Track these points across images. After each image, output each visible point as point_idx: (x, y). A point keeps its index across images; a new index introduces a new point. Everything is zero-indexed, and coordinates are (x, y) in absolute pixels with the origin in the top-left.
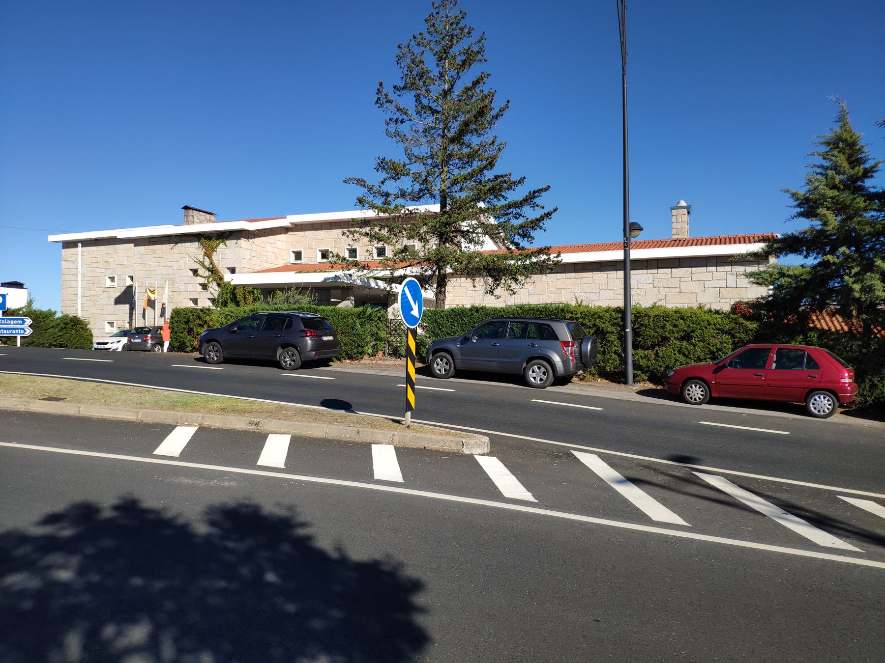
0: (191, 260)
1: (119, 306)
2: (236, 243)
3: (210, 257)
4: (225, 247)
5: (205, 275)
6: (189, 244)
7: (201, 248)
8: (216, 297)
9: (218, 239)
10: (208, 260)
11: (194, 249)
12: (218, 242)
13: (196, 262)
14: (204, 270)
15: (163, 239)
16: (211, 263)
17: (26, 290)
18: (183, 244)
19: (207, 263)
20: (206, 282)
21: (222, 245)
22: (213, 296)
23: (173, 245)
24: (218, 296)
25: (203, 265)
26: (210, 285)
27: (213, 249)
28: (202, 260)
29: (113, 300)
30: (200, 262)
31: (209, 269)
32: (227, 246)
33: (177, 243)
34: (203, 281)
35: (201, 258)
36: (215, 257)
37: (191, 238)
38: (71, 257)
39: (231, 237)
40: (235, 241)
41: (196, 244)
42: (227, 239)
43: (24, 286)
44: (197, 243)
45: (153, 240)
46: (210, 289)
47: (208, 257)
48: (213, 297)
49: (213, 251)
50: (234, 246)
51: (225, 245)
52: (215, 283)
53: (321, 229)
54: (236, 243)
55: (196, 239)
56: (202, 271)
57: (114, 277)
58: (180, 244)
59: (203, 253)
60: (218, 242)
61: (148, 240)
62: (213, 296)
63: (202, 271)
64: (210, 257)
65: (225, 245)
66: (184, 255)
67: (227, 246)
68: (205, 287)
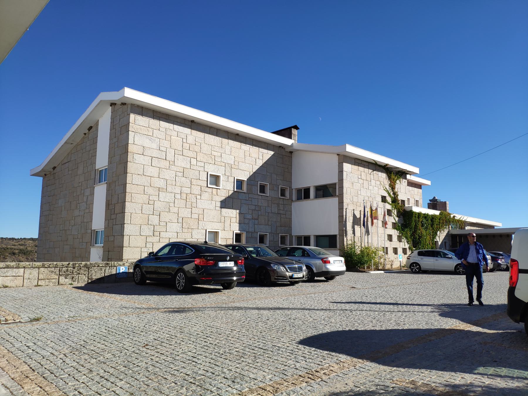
1: (224, 210)
15: (365, 163)
16: (394, 194)
29: (219, 204)
33: (374, 170)
35: (388, 187)
41: (383, 176)
44: (385, 174)
51: (400, 181)
55: (385, 171)
63: (389, 199)
64: (393, 188)
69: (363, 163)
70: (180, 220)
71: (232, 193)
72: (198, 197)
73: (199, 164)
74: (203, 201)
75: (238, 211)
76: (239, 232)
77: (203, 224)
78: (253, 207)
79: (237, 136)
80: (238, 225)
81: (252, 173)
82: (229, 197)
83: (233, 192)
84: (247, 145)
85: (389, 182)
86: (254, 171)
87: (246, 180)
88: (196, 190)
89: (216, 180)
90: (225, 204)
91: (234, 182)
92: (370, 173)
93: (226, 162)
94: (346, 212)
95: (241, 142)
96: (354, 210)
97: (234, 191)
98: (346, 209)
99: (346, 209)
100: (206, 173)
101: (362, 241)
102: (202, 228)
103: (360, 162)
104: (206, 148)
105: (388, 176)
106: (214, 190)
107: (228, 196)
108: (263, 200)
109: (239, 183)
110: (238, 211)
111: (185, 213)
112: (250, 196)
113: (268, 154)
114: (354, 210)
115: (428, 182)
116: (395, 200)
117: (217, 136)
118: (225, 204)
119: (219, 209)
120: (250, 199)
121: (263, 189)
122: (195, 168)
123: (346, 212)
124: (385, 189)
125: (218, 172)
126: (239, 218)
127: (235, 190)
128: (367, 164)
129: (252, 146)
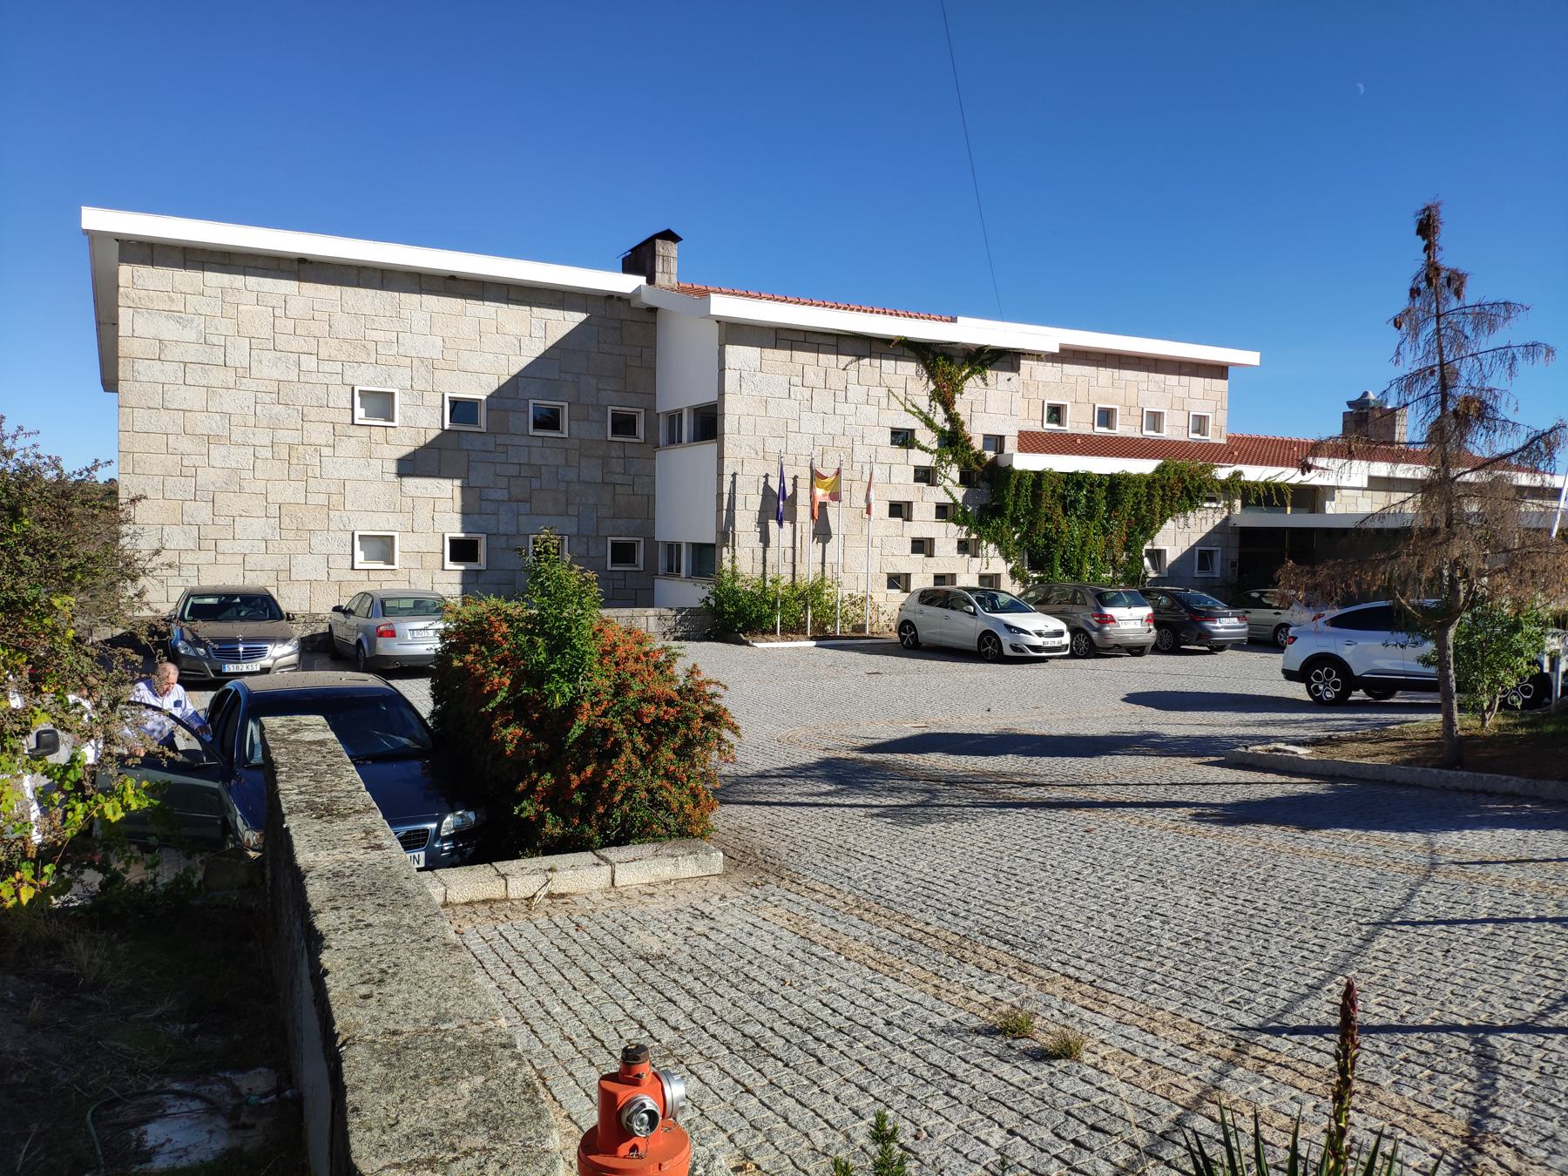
1: (410, 483)
2: (1009, 380)
3: (947, 405)
4: (980, 382)
7: (925, 379)
8: (960, 501)
10: (940, 409)
11: (907, 375)
13: (914, 414)
15: (821, 340)
16: (953, 419)
18: (876, 362)
19: (940, 418)
22: (952, 496)
24: (965, 497)
25: (929, 423)
27: (957, 387)
28: (925, 410)
29: (392, 467)
30: (921, 413)
32: (986, 385)
33: (860, 357)
34: (926, 460)
35: (923, 403)
36: (961, 406)
38: (171, 300)
41: (909, 368)
44: (915, 364)
45: (794, 337)
48: (951, 501)
51: (984, 379)
54: (1009, 380)
55: (913, 354)
57: (392, 394)
61: (772, 335)
62: (952, 496)
63: (926, 437)
64: (947, 405)
65: (984, 379)
67: (986, 385)
68: (925, 476)
70: (274, 510)
71: (438, 437)
72: (326, 451)
73: (326, 367)
74: (341, 460)
75: (458, 482)
76: (462, 535)
77: (345, 520)
78: (513, 470)
79: (452, 283)
80: (459, 516)
81: (506, 378)
82: (428, 447)
83: (438, 432)
84: (487, 303)
85: (932, 387)
86: (515, 370)
87: (484, 398)
88: (319, 434)
89: (381, 404)
90: (410, 466)
91: (443, 407)
92: (842, 366)
93: (414, 354)
94: (734, 482)
95: (465, 296)
96: (766, 476)
97: (443, 429)
98: (734, 475)
99: (734, 475)
100: (349, 389)
101: (798, 559)
102: (342, 528)
104: (343, 325)
105: (927, 367)
106: (378, 434)
107: (422, 444)
108: (548, 450)
109: (462, 409)
110: (458, 482)
111: (288, 492)
113: (566, 321)
114: (766, 476)
115: (1251, 358)
116: (953, 440)
117: (382, 288)
118: (410, 466)
119: (392, 477)
120: (499, 449)
121: (548, 420)
122: (314, 378)
124: (909, 406)
125: (389, 383)
126: (463, 499)
127: (447, 427)
128: (833, 341)
129: (504, 305)
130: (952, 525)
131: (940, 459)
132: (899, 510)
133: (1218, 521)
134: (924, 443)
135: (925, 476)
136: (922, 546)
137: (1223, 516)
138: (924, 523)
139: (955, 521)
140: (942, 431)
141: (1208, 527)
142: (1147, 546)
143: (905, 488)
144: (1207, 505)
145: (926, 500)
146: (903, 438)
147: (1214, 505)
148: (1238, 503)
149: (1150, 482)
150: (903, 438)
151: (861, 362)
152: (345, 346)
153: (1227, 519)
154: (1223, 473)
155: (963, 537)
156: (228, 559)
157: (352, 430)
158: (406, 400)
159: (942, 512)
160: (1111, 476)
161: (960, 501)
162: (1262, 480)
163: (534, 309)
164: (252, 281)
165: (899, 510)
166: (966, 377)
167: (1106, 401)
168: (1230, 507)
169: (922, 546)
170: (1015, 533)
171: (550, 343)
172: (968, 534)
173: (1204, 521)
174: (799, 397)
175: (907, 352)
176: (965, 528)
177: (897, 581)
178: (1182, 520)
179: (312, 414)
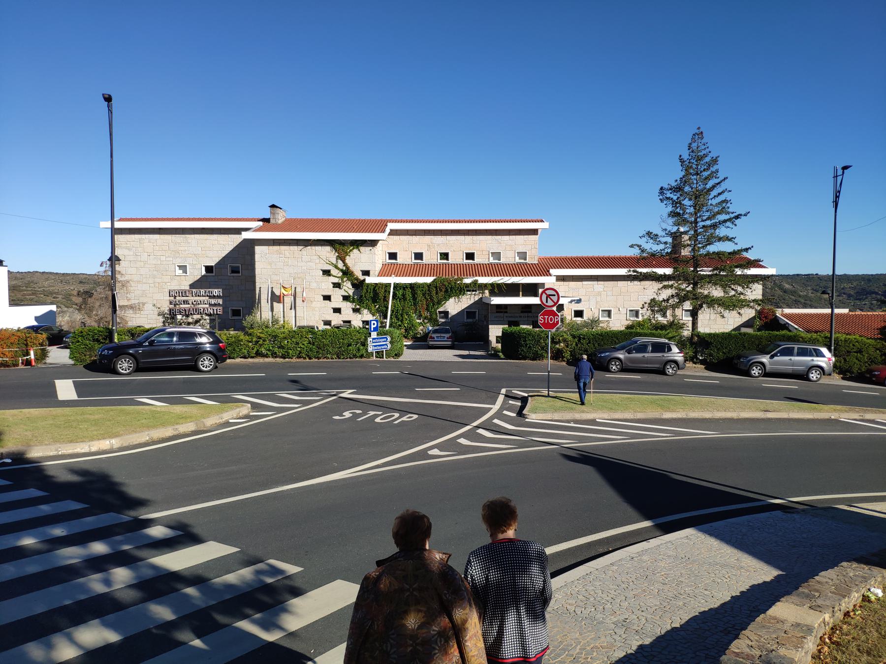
0: (323, 262)
3: (344, 261)
4: (358, 252)
5: (338, 276)
6: (320, 247)
7: (334, 252)
8: (351, 294)
9: (351, 246)
11: (328, 253)
12: (351, 248)
13: (329, 264)
14: (337, 271)
16: (345, 265)
17: (6, 267)
18: (313, 247)
19: (340, 264)
20: (340, 281)
21: (355, 251)
23: (302, 247)
25: (336, 267)
26: (345, 284)
27: (347, 254)
28: (335, 262)
30: (333, 264)
31: (342, 270)
33: (306, 246)
34: (336, 280)
35: (334, 261)
36: (348, 260)
37: (323, 243)
39: (364, 245)
40: (371, 248)
41: (328, 248)
42: (361, 246)
43: (4, 263)
46: (344, 288)
47: (341, 260)
48: (348, 294)
49: (346, 255)
50: (368, 252)
51: (359, 250)
52: (350, 283)
53: (415, 235)
55: (328, 244)
56: (334, 272)
57: (186, 266)
58: (309, 247)
59: (335, 256)
60: (351, 248)
63: (334, 272)
64: (344, 261)
65: (359, 250)
66: (315, 257)
69: (288, 241)
71: (200, 278)
73: (168, 259)
85: (337, 254)
93: (192, 253)
103: (291, 242)
105: (334, 248)
112: (219, 278)
116: (347, 273)
123: (260, 290)
128: (296, 242)
130: (348, 303)
131: (342, 280)
132: (327, 298)
133: (477, 299)
134: (334, 274)
135: (337, 285)
136: (337, 310)
137: (479, 297)
138: (337, 301)
139: (350, 302)
140: (342, 270)
141: (472, 301)
142: (441, 309)
143: (329, 290)
144: (469, 293)
145: (337, 296)
146: (327, 273)
147: (474, 293)
148: (487, 292)
149: (429, 286)
150: (327, 273)
151: (307, 248)
152: (173, 253)
153: (481, 298)
154: (468, 281)
155: (354, 307)
156: (143, 316)
157: (175, 277)
158: (191, 267)
159: (346, 298)
160: (411, 284)
161: (351, 294)
162: (490, 282)
163: (229, 235)
164: (147, 236)
165: (327, 298)
166: (351, 251)
167: (470, 249)
168: (483, 293)
169: (337, 310)
170: (376, 305)
171: (235, 246)
172: (355, 306)
173: (469, 300)
174: (283, 261)
175: (326, 243)
176: (354, 304)
177: (328, 323)
178: (457, 299)
179: (164, 273)
